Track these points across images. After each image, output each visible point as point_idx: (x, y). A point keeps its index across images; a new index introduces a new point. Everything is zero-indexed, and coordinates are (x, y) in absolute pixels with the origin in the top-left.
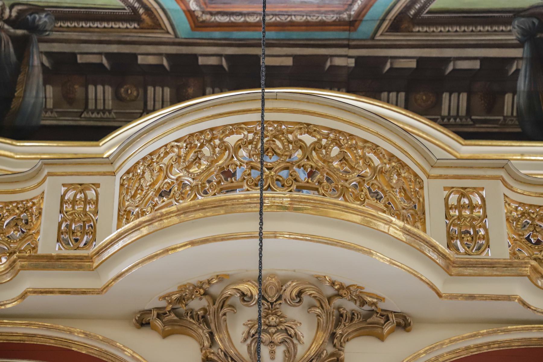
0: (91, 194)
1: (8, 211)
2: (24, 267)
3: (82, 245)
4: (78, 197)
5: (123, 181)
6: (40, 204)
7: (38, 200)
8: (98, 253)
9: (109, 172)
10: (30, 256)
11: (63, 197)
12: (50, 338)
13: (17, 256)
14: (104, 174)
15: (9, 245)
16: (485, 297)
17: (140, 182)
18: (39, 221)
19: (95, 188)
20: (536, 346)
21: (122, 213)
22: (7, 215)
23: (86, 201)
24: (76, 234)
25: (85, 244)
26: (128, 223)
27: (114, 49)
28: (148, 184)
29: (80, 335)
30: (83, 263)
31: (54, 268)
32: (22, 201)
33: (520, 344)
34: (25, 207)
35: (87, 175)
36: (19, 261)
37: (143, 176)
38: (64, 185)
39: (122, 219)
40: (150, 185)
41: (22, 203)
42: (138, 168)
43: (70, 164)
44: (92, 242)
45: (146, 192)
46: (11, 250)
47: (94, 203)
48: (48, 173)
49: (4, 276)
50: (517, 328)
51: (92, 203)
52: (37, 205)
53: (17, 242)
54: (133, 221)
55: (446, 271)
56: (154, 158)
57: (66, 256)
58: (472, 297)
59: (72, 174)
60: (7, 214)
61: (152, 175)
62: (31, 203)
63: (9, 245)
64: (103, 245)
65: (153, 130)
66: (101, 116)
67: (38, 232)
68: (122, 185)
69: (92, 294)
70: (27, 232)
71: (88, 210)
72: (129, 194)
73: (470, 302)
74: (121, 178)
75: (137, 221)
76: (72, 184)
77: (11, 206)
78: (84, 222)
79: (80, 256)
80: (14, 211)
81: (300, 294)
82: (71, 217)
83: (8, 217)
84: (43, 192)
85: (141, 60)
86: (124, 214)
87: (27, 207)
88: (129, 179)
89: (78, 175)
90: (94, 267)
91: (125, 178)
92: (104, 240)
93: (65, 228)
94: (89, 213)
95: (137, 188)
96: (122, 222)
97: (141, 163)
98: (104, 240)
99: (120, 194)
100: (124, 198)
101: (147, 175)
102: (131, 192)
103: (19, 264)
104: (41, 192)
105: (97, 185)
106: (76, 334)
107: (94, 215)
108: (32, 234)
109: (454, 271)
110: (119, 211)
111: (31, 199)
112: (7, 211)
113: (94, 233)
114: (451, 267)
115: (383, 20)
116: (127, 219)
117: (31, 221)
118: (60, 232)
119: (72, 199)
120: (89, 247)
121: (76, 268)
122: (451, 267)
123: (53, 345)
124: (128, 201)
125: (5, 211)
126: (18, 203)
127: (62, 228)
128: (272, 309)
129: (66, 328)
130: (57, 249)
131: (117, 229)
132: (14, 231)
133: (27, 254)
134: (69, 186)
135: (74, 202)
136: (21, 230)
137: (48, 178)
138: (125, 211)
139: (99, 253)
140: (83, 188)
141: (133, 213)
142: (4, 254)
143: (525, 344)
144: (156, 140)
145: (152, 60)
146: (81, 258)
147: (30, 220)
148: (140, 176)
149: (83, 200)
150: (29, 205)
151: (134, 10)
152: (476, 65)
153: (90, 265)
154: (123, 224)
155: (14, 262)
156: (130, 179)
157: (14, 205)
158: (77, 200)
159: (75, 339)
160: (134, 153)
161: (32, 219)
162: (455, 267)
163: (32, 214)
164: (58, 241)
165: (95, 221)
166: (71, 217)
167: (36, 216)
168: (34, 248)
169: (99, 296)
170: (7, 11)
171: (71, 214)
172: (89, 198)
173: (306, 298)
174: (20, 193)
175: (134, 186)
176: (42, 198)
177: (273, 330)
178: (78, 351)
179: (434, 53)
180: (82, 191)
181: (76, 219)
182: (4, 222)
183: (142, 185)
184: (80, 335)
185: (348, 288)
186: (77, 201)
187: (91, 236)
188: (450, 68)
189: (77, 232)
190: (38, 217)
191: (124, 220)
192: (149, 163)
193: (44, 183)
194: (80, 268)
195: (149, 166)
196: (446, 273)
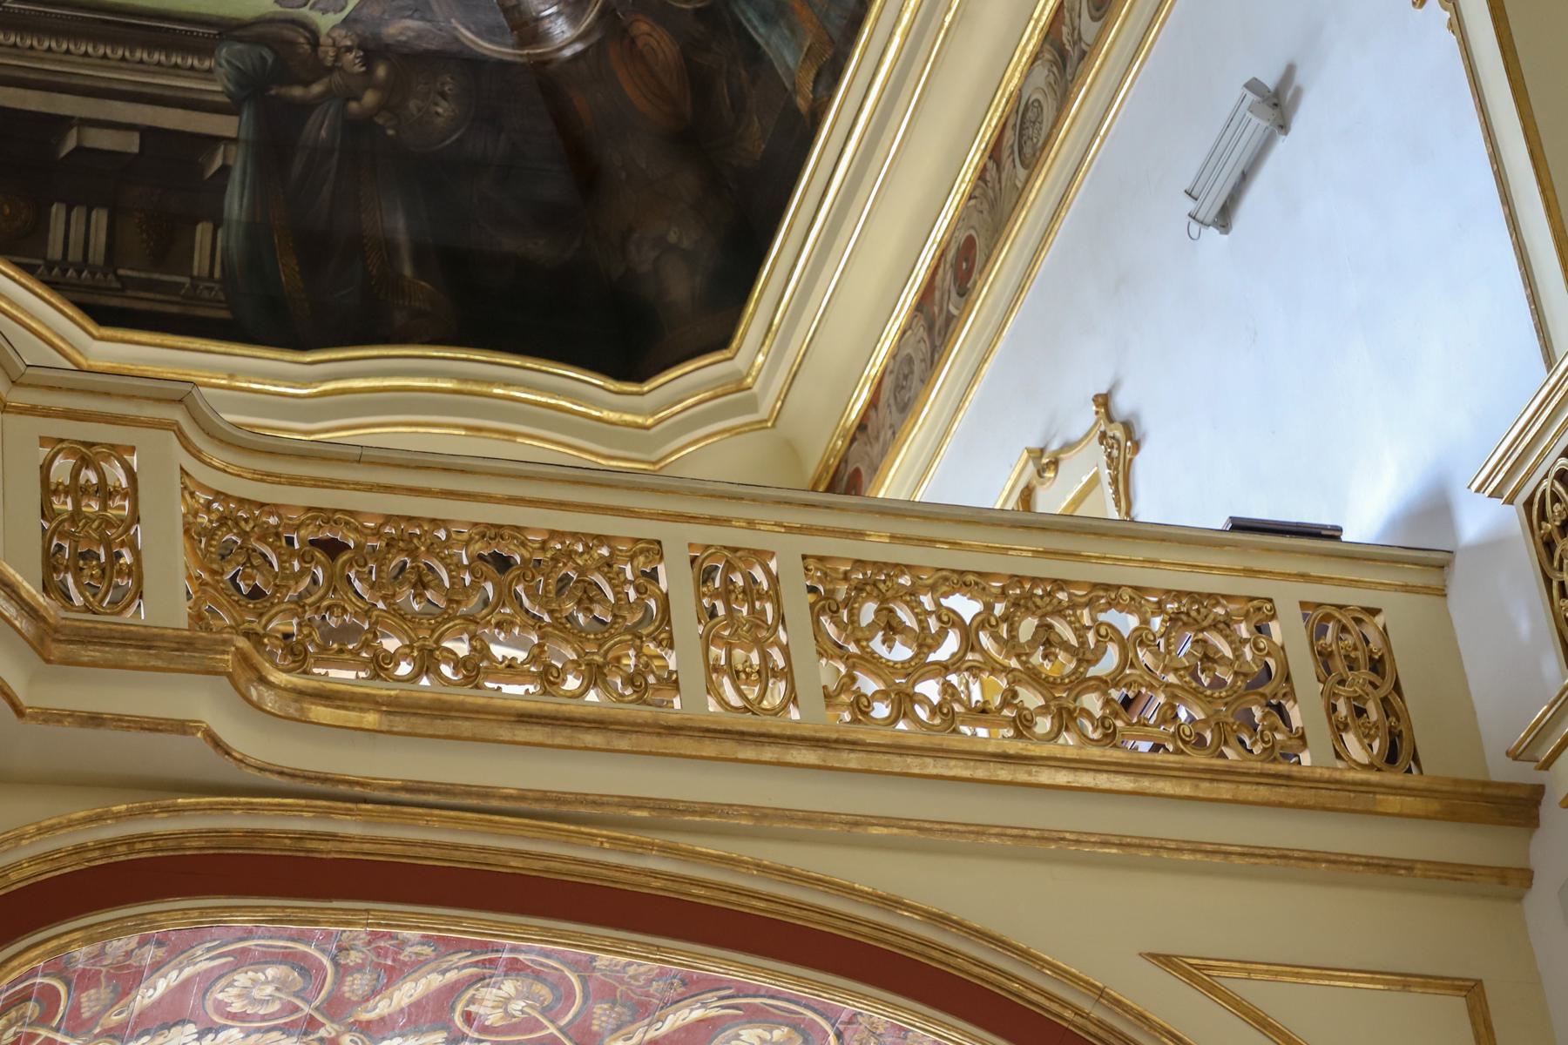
16: (129, 721)
20: (240, 851)
33: (202, 843)
50: (198, 804)
55: (35, 648)
58: (95, 720)
73: (90, 733)
109: (57, 650)
114: (48, 641)
122: (48, 641)
143: (213, 844)
162: (60, 641)
196: (36, 655)
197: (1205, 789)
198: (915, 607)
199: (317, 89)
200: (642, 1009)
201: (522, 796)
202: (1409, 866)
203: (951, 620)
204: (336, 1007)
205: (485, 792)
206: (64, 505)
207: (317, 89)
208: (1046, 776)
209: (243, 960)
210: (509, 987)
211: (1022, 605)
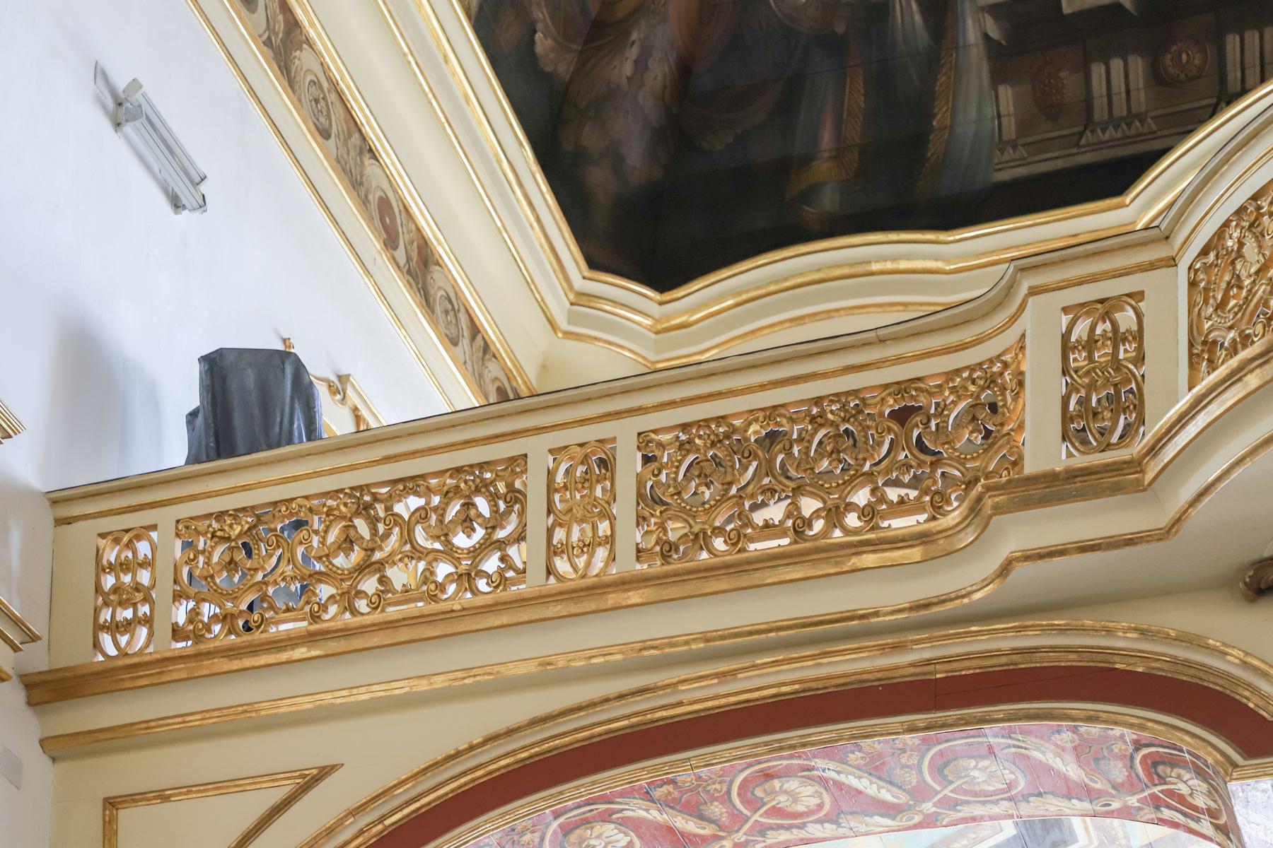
0: (1126, 319)
1: (954, 390)
2: (1001, 508)
3: (1115, 439)
4: (1098, 331)
5: (1195, 274)
6: (1019, 363)
7: (1013, 354)
8: (1152, 448)
9: (1162, 260)
10: (1009, 482)
11: (1066, 337)
13: (983, 487)
14: (1152, 266)
15: (963, 465)
17: (1234, 269)
18: (1021, 401)
19: (1133, 303)
21: (1198, 348)
22: (953, 402)
23: (1117, 338)
24: (1100, 417)
25: (1121, 437)
26: (1214, 370)
28: (1253, 270)
29: (1129, 635)
30: (1122, 477)
31: (1061, 499)
32: (980, 364)
34: (988, 375)
35: (1115, 277)
36: (990, 497)
37: (1240, 255)
38: (1066, 310)
39: (1198, 363)
40: (1257, 272)
41: (981, 368)
42: (1227, 236)
43: (1076, 258)
44: (1138, 428)
45: (1250, 291)
46: (969, 476)
47: (1134, 338)
48: (1030, 288)
49: (963, 534)
51: (1130, 338)
52: (1013, 367)
53: (979, 455)
54: (1223, 363)
56: (1263, 204)
57: (1086, 468)
59: (1080, 282)
60: (952, 398)
61: (1260, 247)
62: (999, 365)
63: (963, 465)
64: (1163, 430)
65: (1258, 137)
66: (1137, 128)
67: (1021, 427)
68: (1193, 284)
69: (1148, 542)
70: (998, 431)
71: (1121, 356)
72: (1211, 301)
74: (1190, 268)
75: (1234, 362)
76: (1083, 305)
77: (958, 380)
78: (1115, 385)
79: (1114, 463)
80: (966, 389)
82: (1087, 380)
83: (956, 405)
84: (1023, 335)
86: (1203, 351)
87: (993, 374)
88: (1207, 268)
89: (1095, 281)
90: (1146, 483)
91: (1198, 266)
92: (1165, 419)
93: (1078, 407)
94: (1125, 363)
95: (1229, 283)
96: (1199, 371)
97: (1234, 223)
98: (1165, 419)
99: (1191, 306)
100: (1199, 314)
101: (1250, 249)
102: (1214, 297)
103: (989, 502)
104: (1019, 337)
105: (1138, 296)
106: (1120, 634)
107: (1135, 366)
108: (1008, 434)
110: (1191, 345)
111: (999, 356)
112: (951, 393)
113: (1139, 407)
116: (1210, 361)
117: (1004, 406)
118: (1066, 418)
119: (1085, 338)
120: (1133, 438)
121: (1108, 492)
123: (1074, 664)
124: (1209, 319)
125: (947, 393)
126: (972, 369)
127: (1071, 408)
129: (1098, 625)
130: (1064, 457)
131: (1190, 390)
132: (971, 432)
133: (1004, 479)
134: (1076, 310)
135: (1090, 344)
136: (985, 427)
137: (1031, 300)
138: (1205, 343)
139: (1154, 449)
140: (1107, 308)
141: (1222, 345)
142: (954, 488)
144: (1264, 160)
146: (1116, 467)
147: (1001, 404)
148: (1234, 255)
149: (1110, 335)
150: (995, 369)
153: (1137, 479)
154: (1201, 376)
155: (979, 499)
156: (1211, 265)
157: (965, 375)
158: (1096, 338)
159: (1120, 644)
160: (1217, 201)
161: (1004, 400)
163: (1003, 389)
164: (1064, 439)
165: (1139, 378)
166: (1087, 380)
167: (1013, 391)
168: (1015, 463)
169: (1160, 544)
171: (1088, 373)
172: (1122, 330)
174: (975, 345)
175: (1221, 280)
176: (1022, 348)
178: (1128, 668)
180: (1107, 316)
181: (1099, 383)
182: (948, 416)
183: (1238, 276)
184: (1129, 635)
186: (1097, 341)
187: (1134, 415)
189: (1102, 412)
190: (1017, 393)
191: (1204, 364)
192: (1253, 218)
193: (1023, 315)
194: (1116, 489)
195: (1252, 225)
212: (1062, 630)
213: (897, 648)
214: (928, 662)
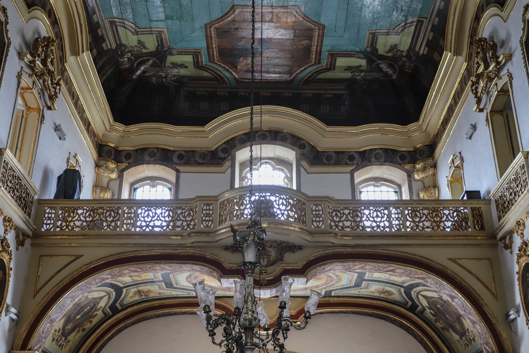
12: (200, 254)
27: (209, 90)
81: (271, 245)
85: (218, 93)
115: (301, 81)
128: (264, 248)
145: (222, 93)
151: (216, 77)
152: (332, 96)
170: (173, 78)
173: (272, 246)
177: (264, 255)
179: (318, 92)
185: (285, 242)
188: (323, 97)
197: (455, 238)
198: (420, 213)
199: (357, 86)
200: (385, 268)
201: (369, 245)
202: (482, 245)
203: (424, 214)
204: (349, 268)
205: (365, 245)
206: (314, 213)
207: (357, 86)
208: (434, 238)
209: (337, 266)
210: (369, 266)
211: (433, 211)
212: (199, 251)
213: (176, 250)
214: (180, 252)
